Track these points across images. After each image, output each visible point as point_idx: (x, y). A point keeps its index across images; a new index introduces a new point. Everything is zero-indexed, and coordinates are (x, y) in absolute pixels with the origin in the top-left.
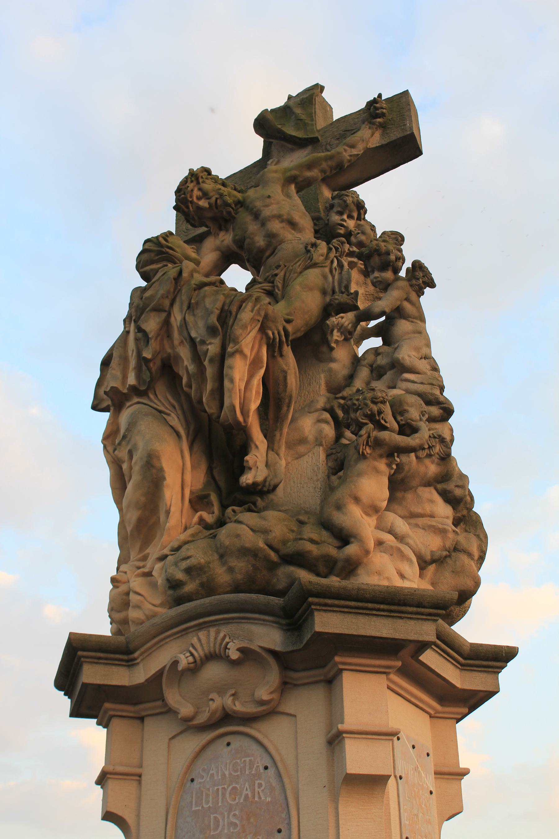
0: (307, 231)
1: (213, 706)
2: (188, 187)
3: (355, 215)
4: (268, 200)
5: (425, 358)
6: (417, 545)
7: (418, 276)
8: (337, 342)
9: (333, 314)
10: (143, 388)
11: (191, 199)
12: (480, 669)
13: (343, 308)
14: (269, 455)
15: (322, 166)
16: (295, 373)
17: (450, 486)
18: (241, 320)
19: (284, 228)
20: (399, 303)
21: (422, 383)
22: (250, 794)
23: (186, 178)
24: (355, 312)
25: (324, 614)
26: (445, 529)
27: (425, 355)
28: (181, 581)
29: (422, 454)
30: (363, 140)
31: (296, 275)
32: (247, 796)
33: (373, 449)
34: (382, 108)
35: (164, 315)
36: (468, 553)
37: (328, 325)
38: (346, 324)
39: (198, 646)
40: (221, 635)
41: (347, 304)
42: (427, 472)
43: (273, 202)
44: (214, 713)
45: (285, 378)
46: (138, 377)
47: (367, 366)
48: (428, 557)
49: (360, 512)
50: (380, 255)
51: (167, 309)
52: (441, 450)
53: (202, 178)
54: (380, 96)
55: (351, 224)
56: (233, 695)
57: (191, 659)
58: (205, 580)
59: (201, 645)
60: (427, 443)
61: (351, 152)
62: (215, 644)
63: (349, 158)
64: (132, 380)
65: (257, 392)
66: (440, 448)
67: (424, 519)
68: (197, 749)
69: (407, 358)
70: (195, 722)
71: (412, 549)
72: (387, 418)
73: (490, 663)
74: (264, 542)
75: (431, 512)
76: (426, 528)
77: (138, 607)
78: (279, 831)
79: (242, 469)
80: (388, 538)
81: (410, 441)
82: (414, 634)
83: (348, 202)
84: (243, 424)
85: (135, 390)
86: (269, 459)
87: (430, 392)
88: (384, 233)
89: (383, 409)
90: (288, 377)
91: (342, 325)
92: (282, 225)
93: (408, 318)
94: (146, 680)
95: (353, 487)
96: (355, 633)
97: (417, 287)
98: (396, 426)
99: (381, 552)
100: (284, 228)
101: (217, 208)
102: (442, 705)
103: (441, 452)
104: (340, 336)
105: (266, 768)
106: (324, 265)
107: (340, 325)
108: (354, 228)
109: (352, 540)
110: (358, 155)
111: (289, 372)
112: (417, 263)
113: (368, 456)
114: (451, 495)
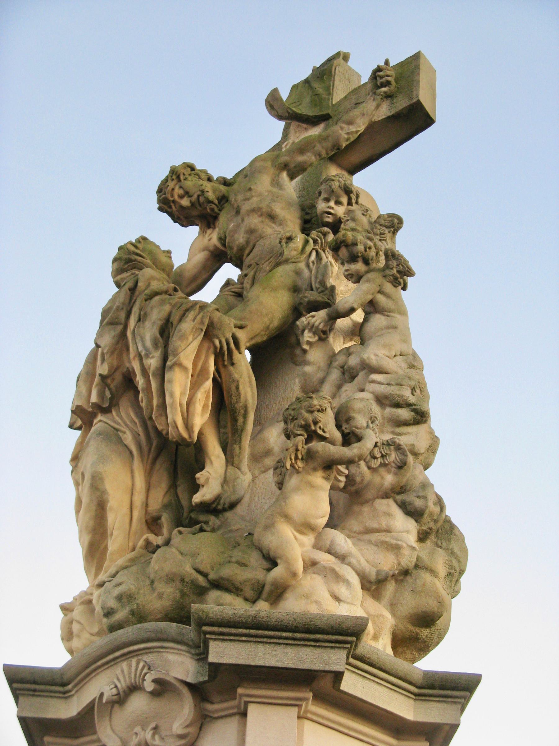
0: (289, 222)
2: (168, 186)
3: (345, 200)
4: (248, 194)
5: (400, 355)
6: (360, 564)
7: (391, 265)
8: (308, 343)
9: (304, 313)
10: (106, 405)
11: (172, 199)
12: (437, 699)
13: (315, 307)
14: (229, 470)
15: (315, 149)
16: (250, 382)
17: (410, 498)
18: (180, 331)
19: (262, 222)
20: (370, 297)
21: (388, 384)
23: (167, 177)
24: (326, 310)
25: (220, 643)
26: (398, 545)
27: (401, 352)
28: (112, 609)
29: (375, 464)
30: (364, 115)
31: (265, 274)
33: (306, 462)
34: (388, 76)
35: (120, 327)
36: (431, 570)
37: (297, 325)
38: (317, 324)
39: (121, 678)
41: (317, 302)
42: (382, 483)
43: (253, 194)
45: (237, 388)
46: (101, 395)
47: (339, 368)
48: (373, 577)
49: (291, 531)
50: (347, 246)
52: (398, 458)
53: (184, 174)
54: (387, 62)
55: (340, 211)
57: (114, 691)
58: (135, 607)
59: (124, 676)
60: (380, 451)
61: (349, 129)
62: (136, 675)
63: (346, 136)
64: (94, 398)
65: (205, 407)
66: (397, 456)
67: (380, 534)
69: (373, 357)
71: (354, 569)
72: (326, 427)
73: (449, 693)
74: (192, 566)
75: (387, 526)
76: (379, 545)
77: (78, 636)
79: (195, 488)
80: (324, 558)
81: (346, 451)
82: (320, 663)
83: (333, 187)
84: (189, 440)
86: (228, 474)
87: (398, 393)
89: (320, 419)
90: (241, 387)
91: (313, 326)
92: (260, 219)
93: (383, 312)
94: (79, 714)
95: (284, 504)
96: (253, 663)
97: (391, 277)
98: (338, 435)
99: (314, 573)
100: (262, 222)
101: (200, 205)
102: (398, 739)
103: (397, 460)
104: (313, 336)
106: (299, 260)
107: (310, 325)
108: (344, 214)
109: (279, 561)
110: (357, 132)
111: (241, 381)
112: (389, 251)
113: (301, 470)
114: (411, 506)
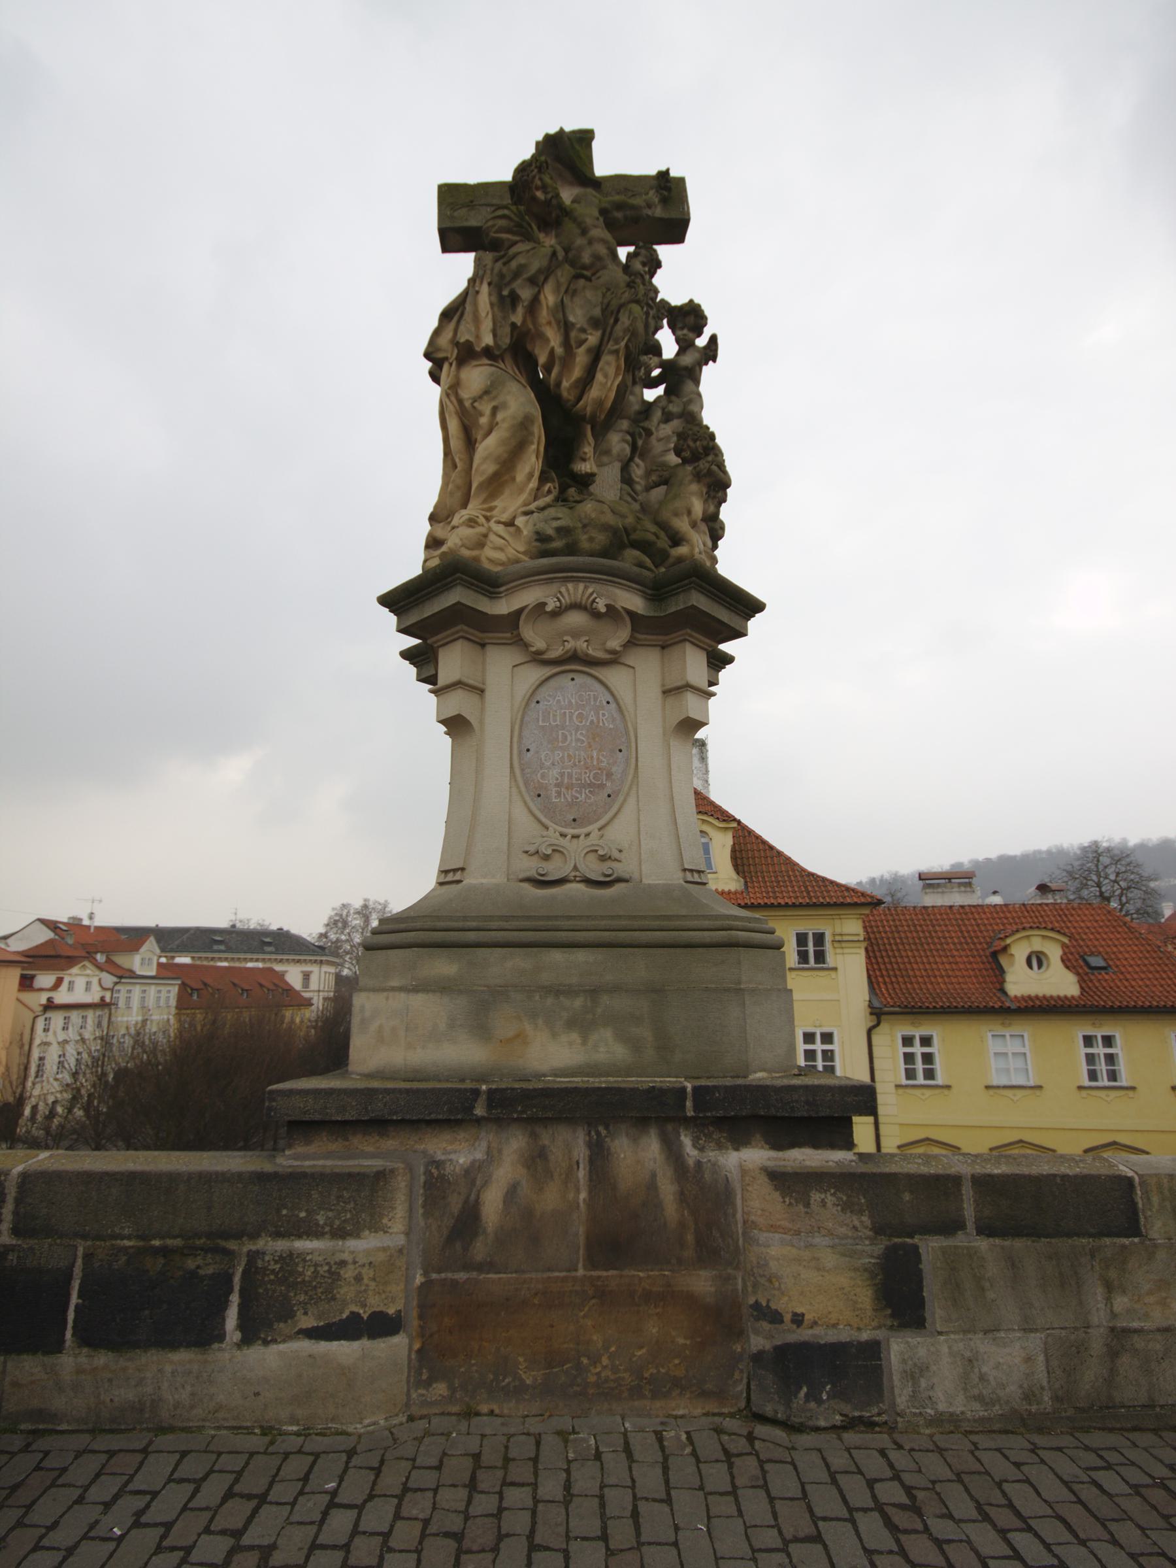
1: (568, 646)
10: (497, 353)
32: (592, 721)
39: (566, 595)
40: (590, 590)
44: (567, 652)
51: (540, 284)
56: (586, 641)
64: (488, 340)
68: (544, 678)
70: (545, 657)
78: (620, 751)
85: (488, 352)
105: (608, 703)
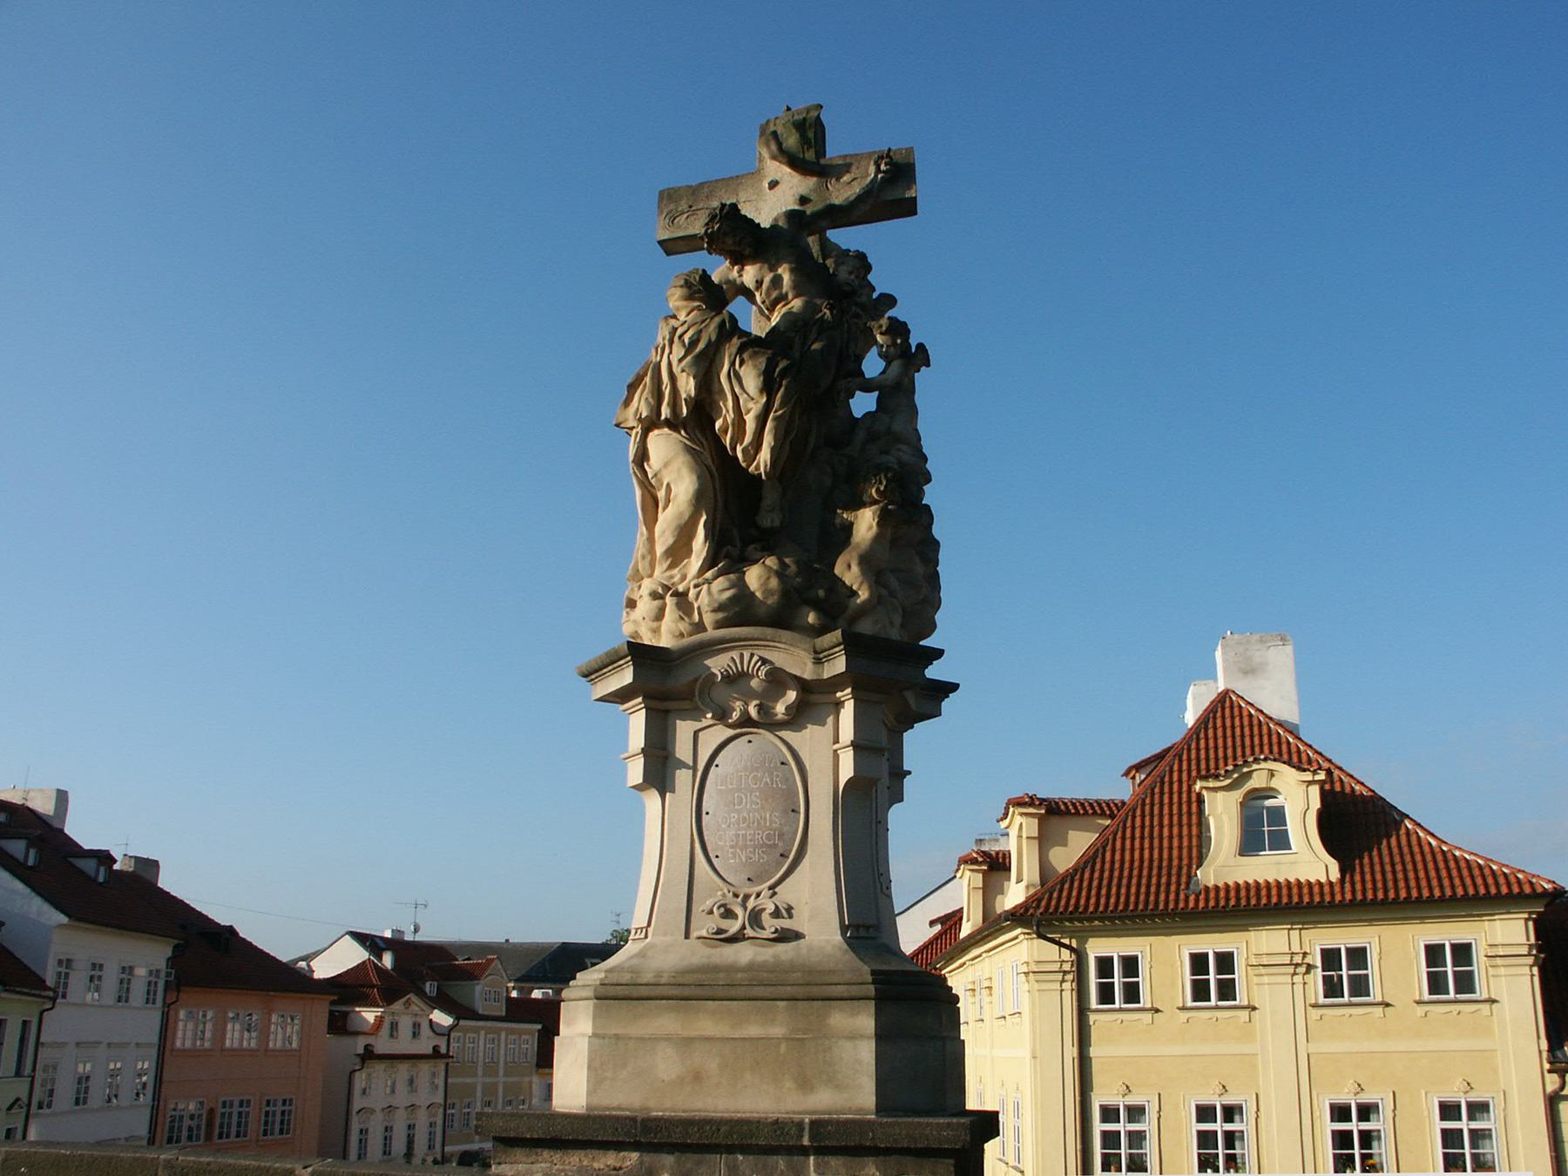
22: (770, 783)
88: (881, 295)
